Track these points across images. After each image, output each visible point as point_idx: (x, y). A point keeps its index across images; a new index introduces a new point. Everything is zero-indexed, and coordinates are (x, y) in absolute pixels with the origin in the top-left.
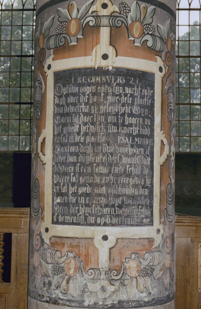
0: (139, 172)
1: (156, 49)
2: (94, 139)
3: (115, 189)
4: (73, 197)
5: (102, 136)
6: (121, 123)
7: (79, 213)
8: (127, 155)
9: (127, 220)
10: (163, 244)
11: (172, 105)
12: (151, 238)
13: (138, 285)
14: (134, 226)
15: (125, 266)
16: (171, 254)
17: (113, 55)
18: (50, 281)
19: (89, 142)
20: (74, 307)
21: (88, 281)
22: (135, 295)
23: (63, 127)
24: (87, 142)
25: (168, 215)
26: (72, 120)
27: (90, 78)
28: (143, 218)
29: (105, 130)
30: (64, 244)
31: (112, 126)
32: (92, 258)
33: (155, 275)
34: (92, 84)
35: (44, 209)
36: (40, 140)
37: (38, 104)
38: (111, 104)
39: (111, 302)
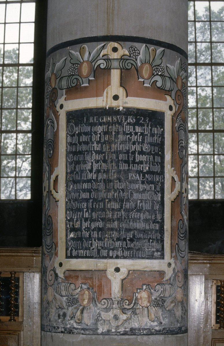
0: (149, 208)
1: (165, 89)
2: (106, 176)
3: (127, 223)
4: (86, 232)
5: (114, 173)
6: (132, 161)
7: (92, 246)
8: (138, 191)
9: (138, 253)
10: (175, 277)
11: (184, 142)
12: (161, 271)
13: (149, 314)
14: (145, 259)
15: (136, 296)
16: (183, 288)
17: (123, 95)
18: (65, 312)
19: (101, 179)
20: (88, 334)
21: (101, 310)
22: (147, 323)
23: (76, 165)
24: (99, 179)
25: (179, 250)
26: (84, 158)
27: (102, 118)
28: (154, 252)
29: (116, 167)
30: (78, 277)
31: (124, 164)
32: (105, 288)
33: (166, 306)
34: (104, 124)
35: (58, 245)
36: (53, 177)
37: (49, 142)
38: (122, 142)
39: (123, 330)
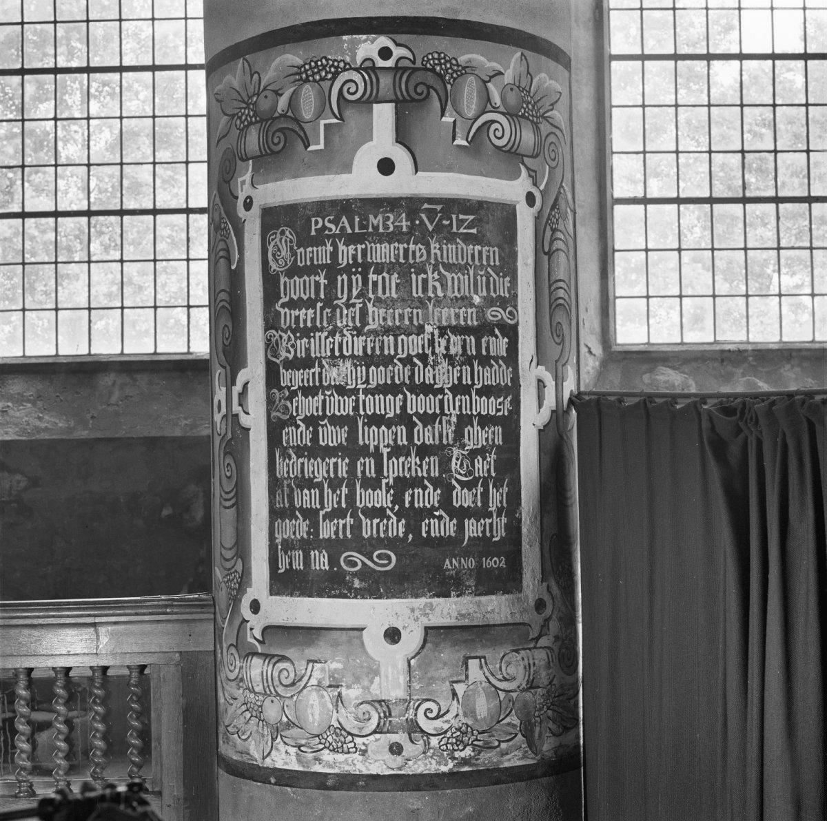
36: (237, 389)
